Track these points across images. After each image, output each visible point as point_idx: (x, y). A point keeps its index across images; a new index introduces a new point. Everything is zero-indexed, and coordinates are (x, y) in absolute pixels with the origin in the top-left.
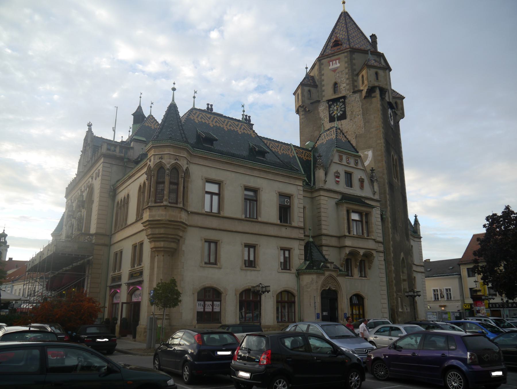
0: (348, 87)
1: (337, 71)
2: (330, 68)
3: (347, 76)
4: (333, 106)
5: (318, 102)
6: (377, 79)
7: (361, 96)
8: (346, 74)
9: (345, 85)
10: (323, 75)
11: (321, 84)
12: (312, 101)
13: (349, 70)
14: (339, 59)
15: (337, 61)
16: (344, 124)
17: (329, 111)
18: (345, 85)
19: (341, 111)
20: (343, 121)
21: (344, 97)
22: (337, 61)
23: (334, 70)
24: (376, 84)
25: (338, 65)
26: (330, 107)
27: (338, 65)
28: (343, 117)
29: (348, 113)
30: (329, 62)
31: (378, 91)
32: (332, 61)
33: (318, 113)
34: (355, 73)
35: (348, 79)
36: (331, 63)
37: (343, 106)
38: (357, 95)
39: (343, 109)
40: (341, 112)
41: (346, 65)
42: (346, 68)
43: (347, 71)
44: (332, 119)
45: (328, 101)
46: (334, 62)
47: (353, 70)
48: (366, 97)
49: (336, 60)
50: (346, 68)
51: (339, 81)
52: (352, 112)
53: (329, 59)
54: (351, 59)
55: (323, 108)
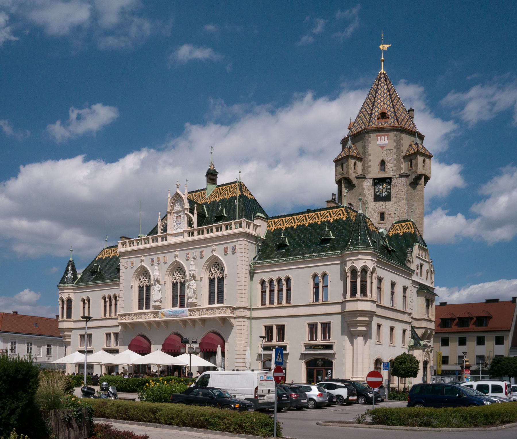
0: (395, 168)
1: (385, 149)
2: (379, 142)
3: (395, 156)
5: (364, 177)
6: (424, 166)
8: (395, 154)
9: (392, 165)
12: (357, 175)
13: (397, 150)
14: (388, 135)
15: (386, 137)
16: (388, 206)
17: (374, 190)
18: (392, 165)
19: (386, 191)
20: (387, 203)
21: (391, 179)
22: (386, 137)
23: (382, 147)
24: (423, 173)
25: (387, 142)
27: (387, 142)
30: (377, 136)
31: (423, 179)
32: (381, 136)
33: (363, 189)
35: (395, 160)
36: (379, 138)
37: (388, 187)
39: (388, 190)
43: (395, 150)
44: (377, 198)
46: (383, 137)
51: (386, 160)
55: (368, 184)
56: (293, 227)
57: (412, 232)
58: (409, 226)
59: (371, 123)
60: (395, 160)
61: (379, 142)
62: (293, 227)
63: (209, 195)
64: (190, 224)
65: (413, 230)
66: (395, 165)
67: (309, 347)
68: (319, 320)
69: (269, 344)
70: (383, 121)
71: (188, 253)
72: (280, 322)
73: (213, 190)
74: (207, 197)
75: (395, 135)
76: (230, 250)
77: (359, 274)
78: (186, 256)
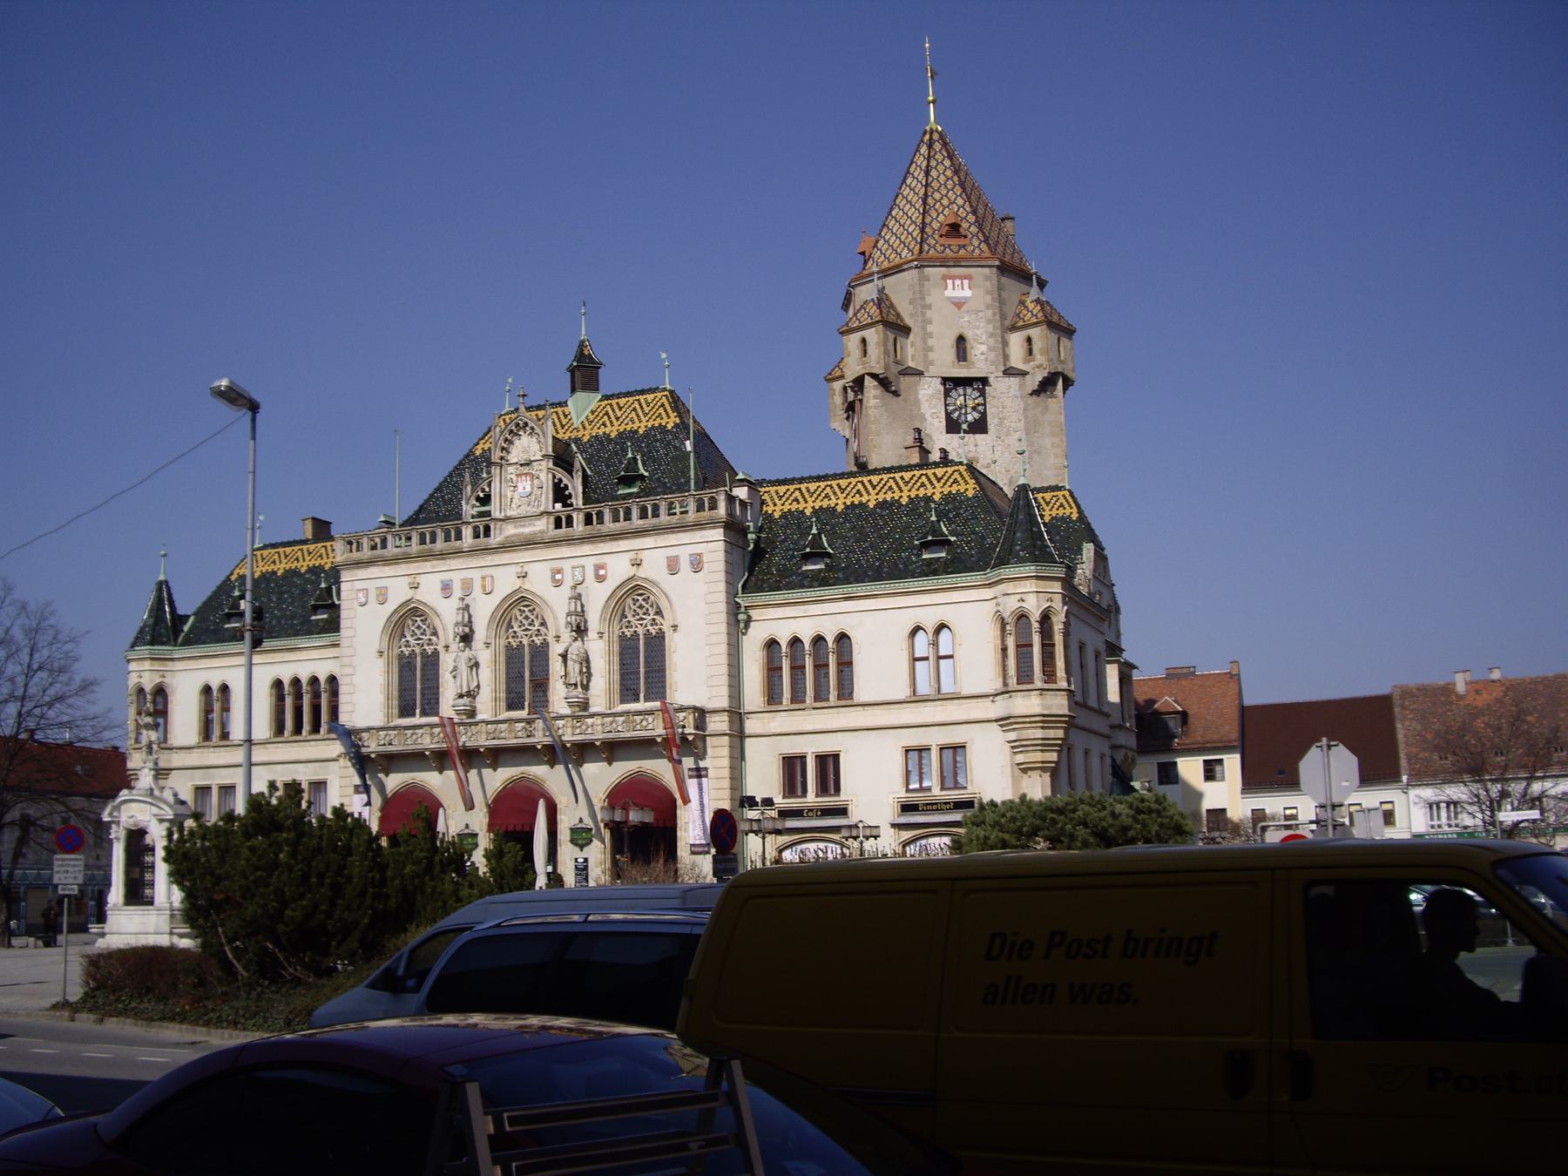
0: (992, 356)
1: (964, 308)
2: (949, 293)
3: (990, 328)
4: (953, 393)
7: (1021, 387)
9: (983, 348)
10: (930, 307)
11: (924, 328)
14: (969, 277)
15: (966, 282)
18: (983, 348)
23: (959, 304)
25: (968, 293)
26: (947, 394)
27: (968, 293)
28: (979, 427)
29: (992, 422)
30: (945, 278)
32: (953, 278)
33: (917, 403)
34: (1008, 323)
35: (992, 335)
37: (980, 400)
38: (1014, 381)
40: (976, 415)
41: (988, 299)
42: (988, 307)
43: (989, 313)
45: (945, 380)
46: (958, 282)
47: (1003, 317)
48: (1036, 393)
49: (962, 278)
50: (988, 307)
51: (969, 335)
52: (1001, 424)
53: (944, 269)
54: (1000, 288)
55: (930, 391)
56: (834, 509)
57: (1075, 516)
58: (1062, 500)
59: (926, 247)
60: (992, 335)
61: (949, 293)
62: (834, 509)
63: (583, 418)
64: (560, 494)
65: (1075, 510)
66: (991, 349)
67: (907, 808)
68: (935, 738)
69: (793, 803)
70: (954, 242)
72: (826, 745)
73: (593, 406)
74: (577, 423)
75: (987, 278)
76: (685, 565)
77: (1036, 625)
78: (554, 580)
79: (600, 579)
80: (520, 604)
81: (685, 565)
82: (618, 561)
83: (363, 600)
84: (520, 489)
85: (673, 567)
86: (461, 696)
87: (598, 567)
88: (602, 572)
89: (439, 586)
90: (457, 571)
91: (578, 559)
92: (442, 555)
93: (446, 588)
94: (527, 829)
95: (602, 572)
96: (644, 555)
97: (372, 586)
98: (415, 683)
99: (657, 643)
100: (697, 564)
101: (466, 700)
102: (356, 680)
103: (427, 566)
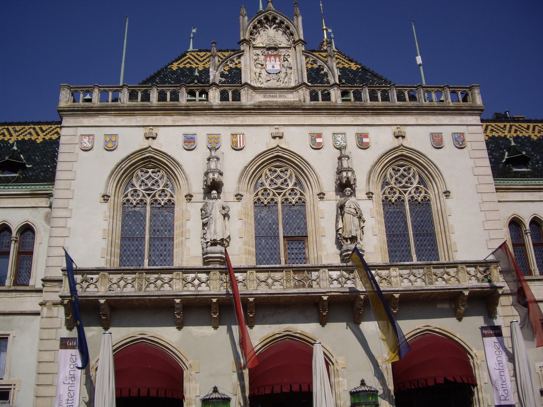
71: (319, 136)
76: (448, 141)
78: (313, 140)
79: (364, 146)
80: (278, 160)
81: (448, 141)
82: (382, 135)
83: (89, 145)
84: (269, 67)
85: (437, 143)
86: (214, 243)
87: (360, 137)
88: (365, 140)
89: (181, 139)
90: (202, 128)
91: (339, 130)
92: (187, 111)
93: (190, 143)
94: (305, 388)
95: (365, 140)
96: (408, 131)
97: (99, 134)
98: (144, 230)
99: (423, 208)
100: (460, 143)
101: (219, 248)
102: (70, 223)
103: (169, 120)
